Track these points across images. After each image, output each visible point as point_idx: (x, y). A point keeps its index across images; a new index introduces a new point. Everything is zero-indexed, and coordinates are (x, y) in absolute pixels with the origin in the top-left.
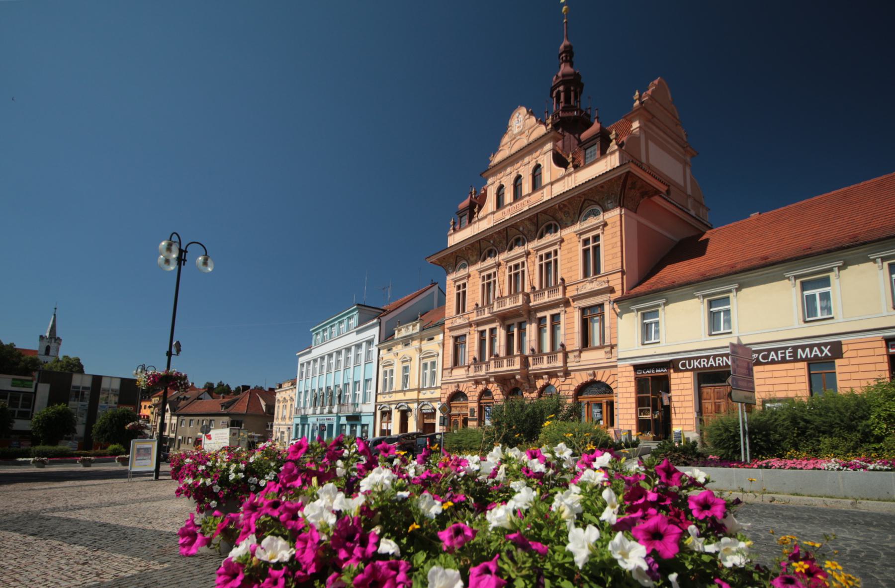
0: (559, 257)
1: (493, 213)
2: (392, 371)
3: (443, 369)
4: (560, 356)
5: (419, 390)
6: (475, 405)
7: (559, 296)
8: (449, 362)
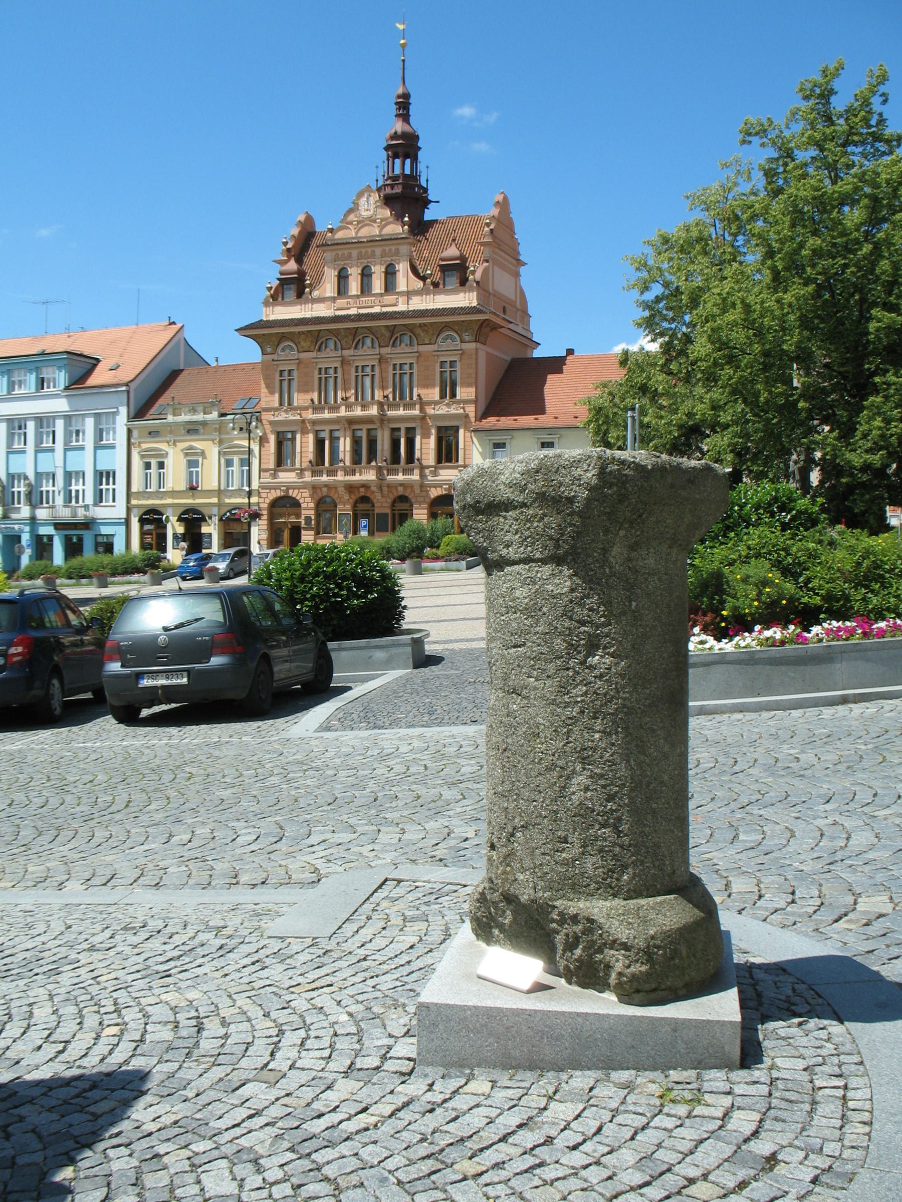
0: (415, 371)
1: (333, 299)
2: (161, 465)
3: (261, 470)
4: (416, 472)
5: (219, 492)
6: (312, 513)
7: (416, 412)
8: (271, 463)
